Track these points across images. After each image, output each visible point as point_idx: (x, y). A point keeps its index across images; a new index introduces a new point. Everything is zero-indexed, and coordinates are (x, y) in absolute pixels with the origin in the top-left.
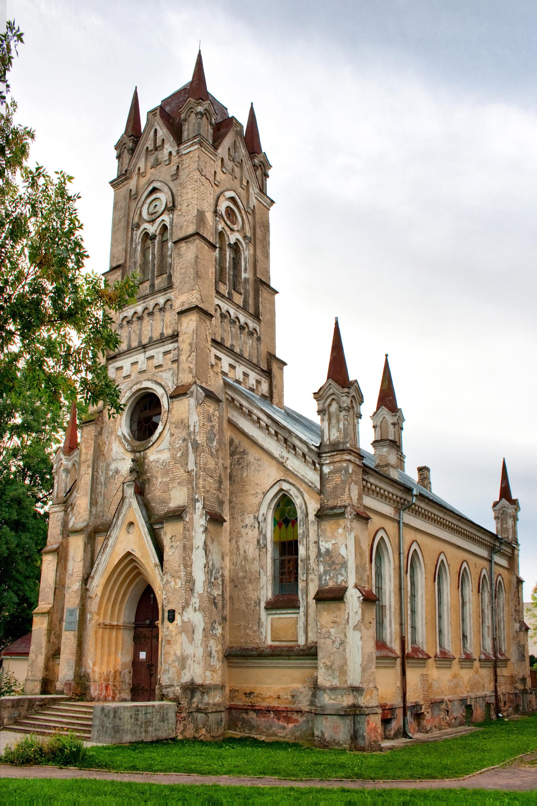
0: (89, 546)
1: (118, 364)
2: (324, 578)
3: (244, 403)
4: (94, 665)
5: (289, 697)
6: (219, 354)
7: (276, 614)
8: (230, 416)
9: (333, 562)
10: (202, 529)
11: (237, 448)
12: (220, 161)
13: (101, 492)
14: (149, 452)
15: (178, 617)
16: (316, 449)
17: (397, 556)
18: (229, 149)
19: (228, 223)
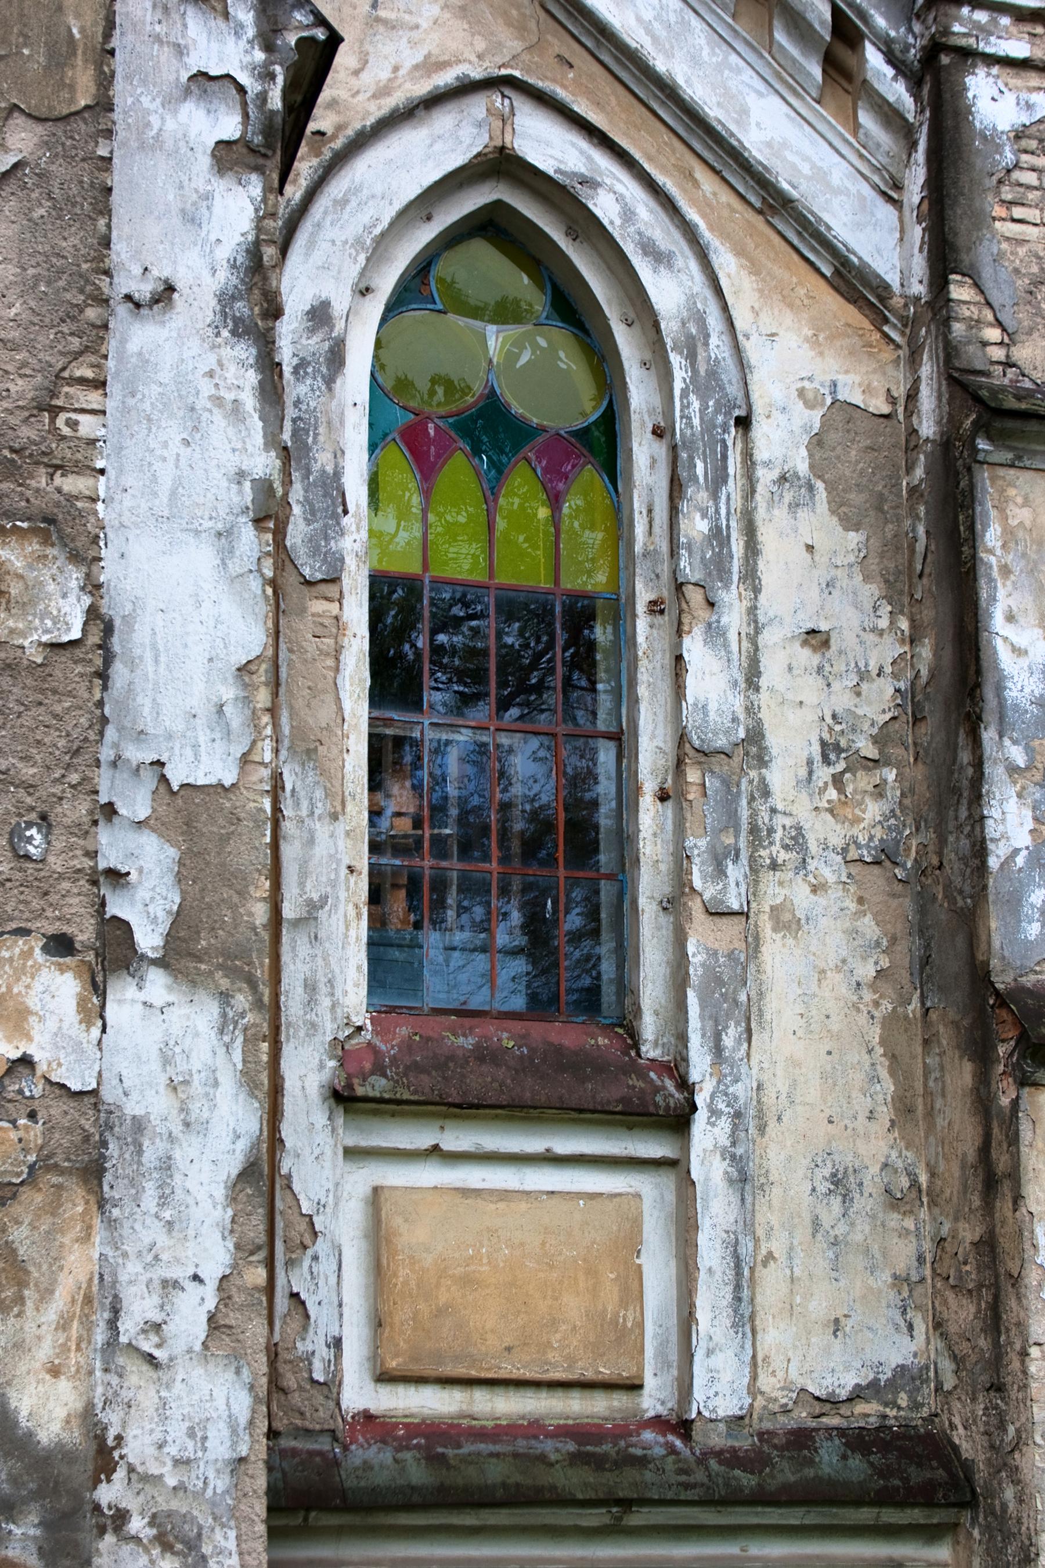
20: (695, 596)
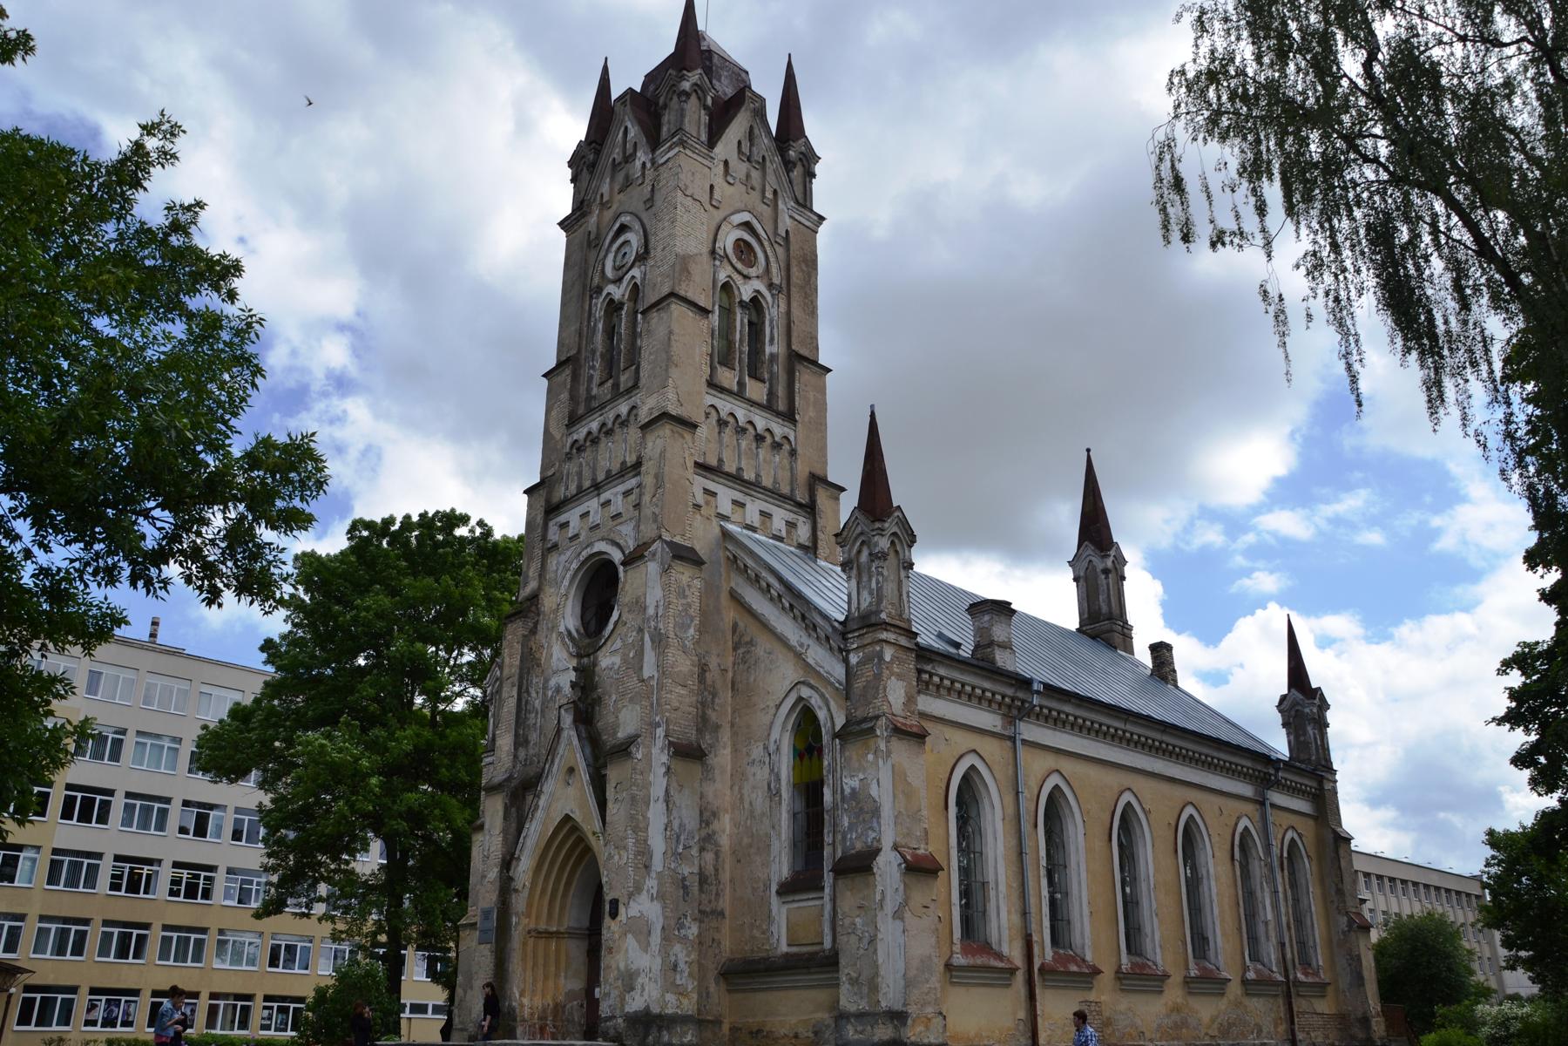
0: (513, 810)
1: (562, 518)
2: (849, 836)
3: (750, 562)
4: (522, 995)
5: (811, 1035)
6: (712, 486)
7: (794, 901)
8: (733, 584)
9: (861, 809)
10: (663, 770)
11: (742, 636)
12: (721, 166)
13: (535, 724)
15: (622, 910)
17: (1009, 799)
18: (739, 142)
19: (739, 266)
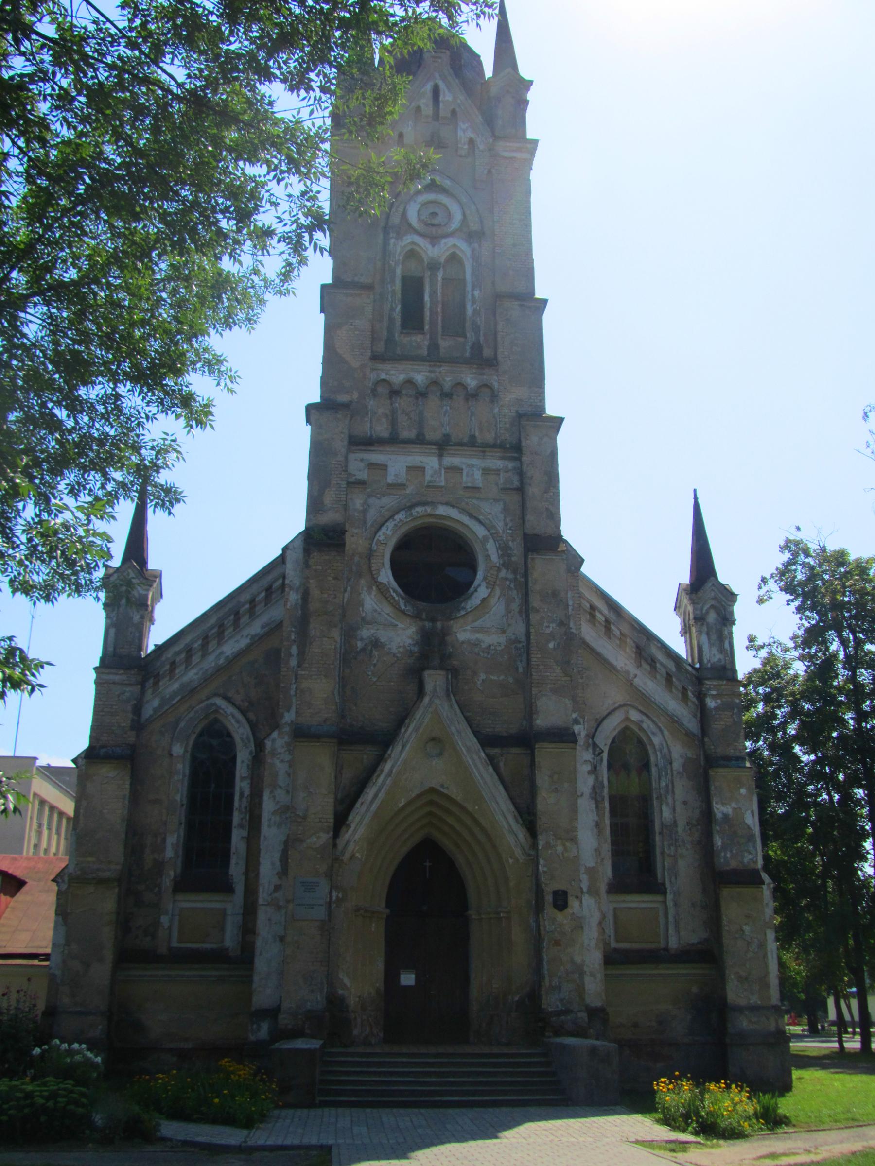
2: (723, 854)
10: (588, 767)
14: (455, 626)
16: (694, 672)
20: (663, 797)
